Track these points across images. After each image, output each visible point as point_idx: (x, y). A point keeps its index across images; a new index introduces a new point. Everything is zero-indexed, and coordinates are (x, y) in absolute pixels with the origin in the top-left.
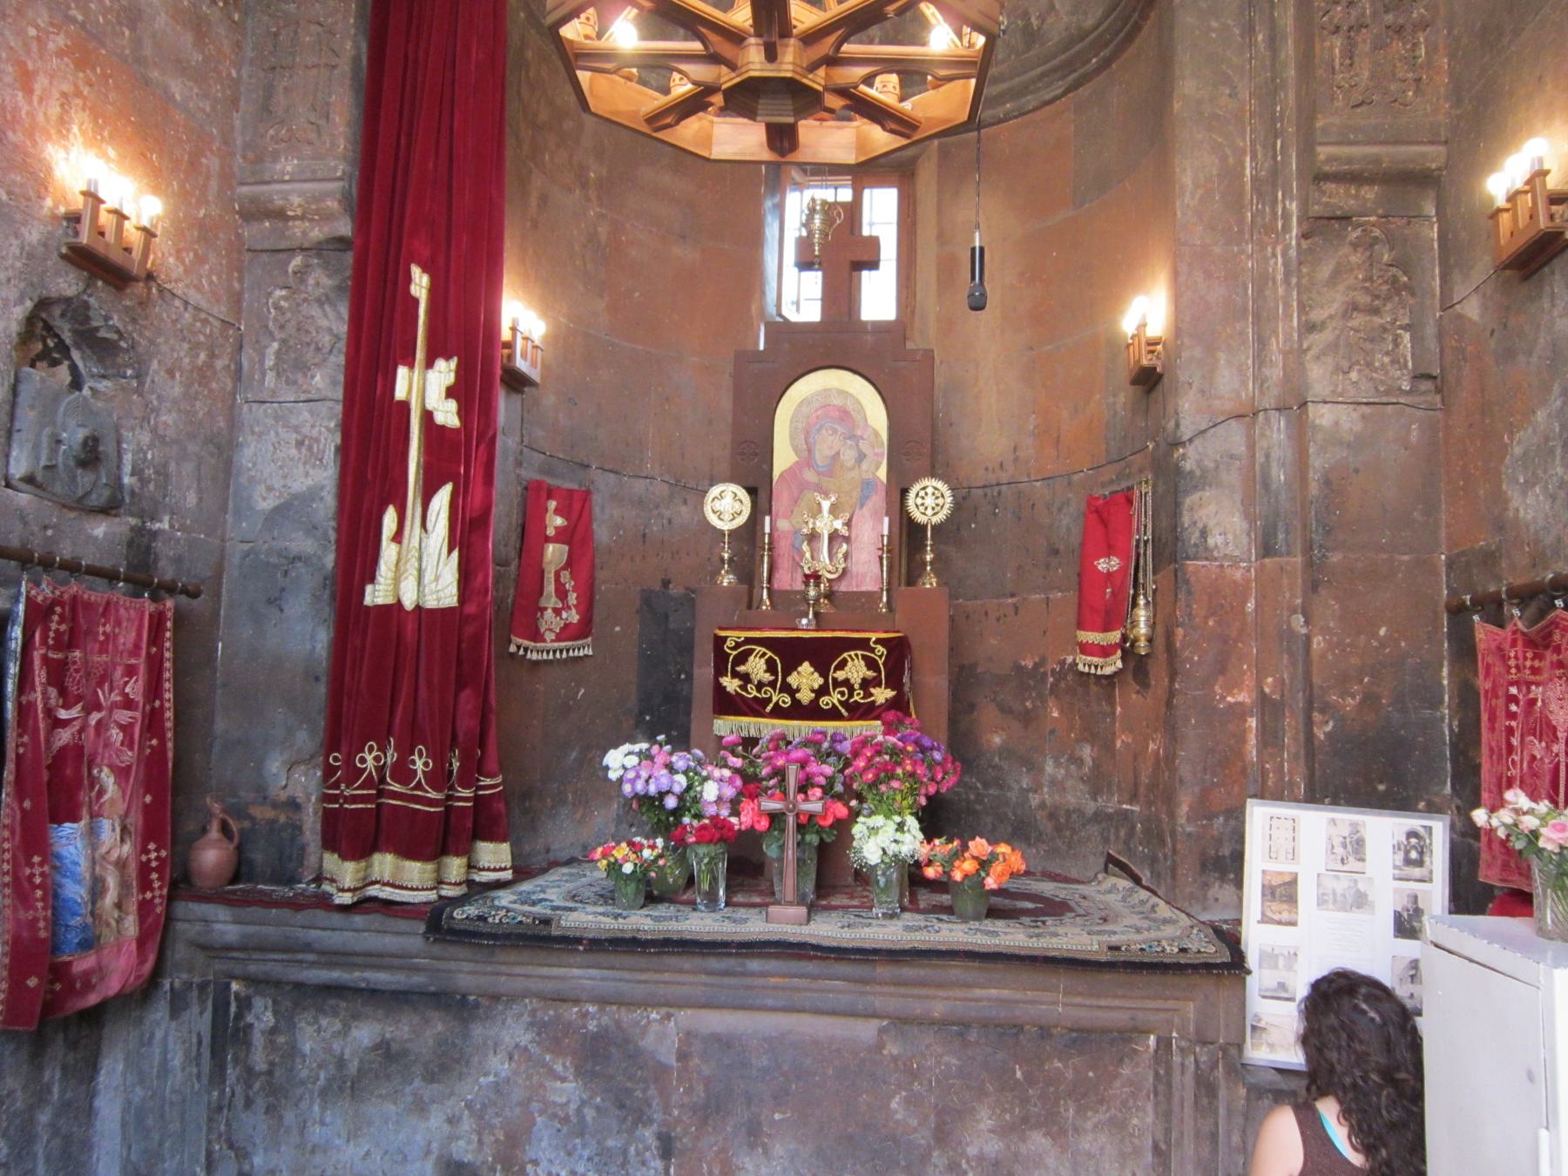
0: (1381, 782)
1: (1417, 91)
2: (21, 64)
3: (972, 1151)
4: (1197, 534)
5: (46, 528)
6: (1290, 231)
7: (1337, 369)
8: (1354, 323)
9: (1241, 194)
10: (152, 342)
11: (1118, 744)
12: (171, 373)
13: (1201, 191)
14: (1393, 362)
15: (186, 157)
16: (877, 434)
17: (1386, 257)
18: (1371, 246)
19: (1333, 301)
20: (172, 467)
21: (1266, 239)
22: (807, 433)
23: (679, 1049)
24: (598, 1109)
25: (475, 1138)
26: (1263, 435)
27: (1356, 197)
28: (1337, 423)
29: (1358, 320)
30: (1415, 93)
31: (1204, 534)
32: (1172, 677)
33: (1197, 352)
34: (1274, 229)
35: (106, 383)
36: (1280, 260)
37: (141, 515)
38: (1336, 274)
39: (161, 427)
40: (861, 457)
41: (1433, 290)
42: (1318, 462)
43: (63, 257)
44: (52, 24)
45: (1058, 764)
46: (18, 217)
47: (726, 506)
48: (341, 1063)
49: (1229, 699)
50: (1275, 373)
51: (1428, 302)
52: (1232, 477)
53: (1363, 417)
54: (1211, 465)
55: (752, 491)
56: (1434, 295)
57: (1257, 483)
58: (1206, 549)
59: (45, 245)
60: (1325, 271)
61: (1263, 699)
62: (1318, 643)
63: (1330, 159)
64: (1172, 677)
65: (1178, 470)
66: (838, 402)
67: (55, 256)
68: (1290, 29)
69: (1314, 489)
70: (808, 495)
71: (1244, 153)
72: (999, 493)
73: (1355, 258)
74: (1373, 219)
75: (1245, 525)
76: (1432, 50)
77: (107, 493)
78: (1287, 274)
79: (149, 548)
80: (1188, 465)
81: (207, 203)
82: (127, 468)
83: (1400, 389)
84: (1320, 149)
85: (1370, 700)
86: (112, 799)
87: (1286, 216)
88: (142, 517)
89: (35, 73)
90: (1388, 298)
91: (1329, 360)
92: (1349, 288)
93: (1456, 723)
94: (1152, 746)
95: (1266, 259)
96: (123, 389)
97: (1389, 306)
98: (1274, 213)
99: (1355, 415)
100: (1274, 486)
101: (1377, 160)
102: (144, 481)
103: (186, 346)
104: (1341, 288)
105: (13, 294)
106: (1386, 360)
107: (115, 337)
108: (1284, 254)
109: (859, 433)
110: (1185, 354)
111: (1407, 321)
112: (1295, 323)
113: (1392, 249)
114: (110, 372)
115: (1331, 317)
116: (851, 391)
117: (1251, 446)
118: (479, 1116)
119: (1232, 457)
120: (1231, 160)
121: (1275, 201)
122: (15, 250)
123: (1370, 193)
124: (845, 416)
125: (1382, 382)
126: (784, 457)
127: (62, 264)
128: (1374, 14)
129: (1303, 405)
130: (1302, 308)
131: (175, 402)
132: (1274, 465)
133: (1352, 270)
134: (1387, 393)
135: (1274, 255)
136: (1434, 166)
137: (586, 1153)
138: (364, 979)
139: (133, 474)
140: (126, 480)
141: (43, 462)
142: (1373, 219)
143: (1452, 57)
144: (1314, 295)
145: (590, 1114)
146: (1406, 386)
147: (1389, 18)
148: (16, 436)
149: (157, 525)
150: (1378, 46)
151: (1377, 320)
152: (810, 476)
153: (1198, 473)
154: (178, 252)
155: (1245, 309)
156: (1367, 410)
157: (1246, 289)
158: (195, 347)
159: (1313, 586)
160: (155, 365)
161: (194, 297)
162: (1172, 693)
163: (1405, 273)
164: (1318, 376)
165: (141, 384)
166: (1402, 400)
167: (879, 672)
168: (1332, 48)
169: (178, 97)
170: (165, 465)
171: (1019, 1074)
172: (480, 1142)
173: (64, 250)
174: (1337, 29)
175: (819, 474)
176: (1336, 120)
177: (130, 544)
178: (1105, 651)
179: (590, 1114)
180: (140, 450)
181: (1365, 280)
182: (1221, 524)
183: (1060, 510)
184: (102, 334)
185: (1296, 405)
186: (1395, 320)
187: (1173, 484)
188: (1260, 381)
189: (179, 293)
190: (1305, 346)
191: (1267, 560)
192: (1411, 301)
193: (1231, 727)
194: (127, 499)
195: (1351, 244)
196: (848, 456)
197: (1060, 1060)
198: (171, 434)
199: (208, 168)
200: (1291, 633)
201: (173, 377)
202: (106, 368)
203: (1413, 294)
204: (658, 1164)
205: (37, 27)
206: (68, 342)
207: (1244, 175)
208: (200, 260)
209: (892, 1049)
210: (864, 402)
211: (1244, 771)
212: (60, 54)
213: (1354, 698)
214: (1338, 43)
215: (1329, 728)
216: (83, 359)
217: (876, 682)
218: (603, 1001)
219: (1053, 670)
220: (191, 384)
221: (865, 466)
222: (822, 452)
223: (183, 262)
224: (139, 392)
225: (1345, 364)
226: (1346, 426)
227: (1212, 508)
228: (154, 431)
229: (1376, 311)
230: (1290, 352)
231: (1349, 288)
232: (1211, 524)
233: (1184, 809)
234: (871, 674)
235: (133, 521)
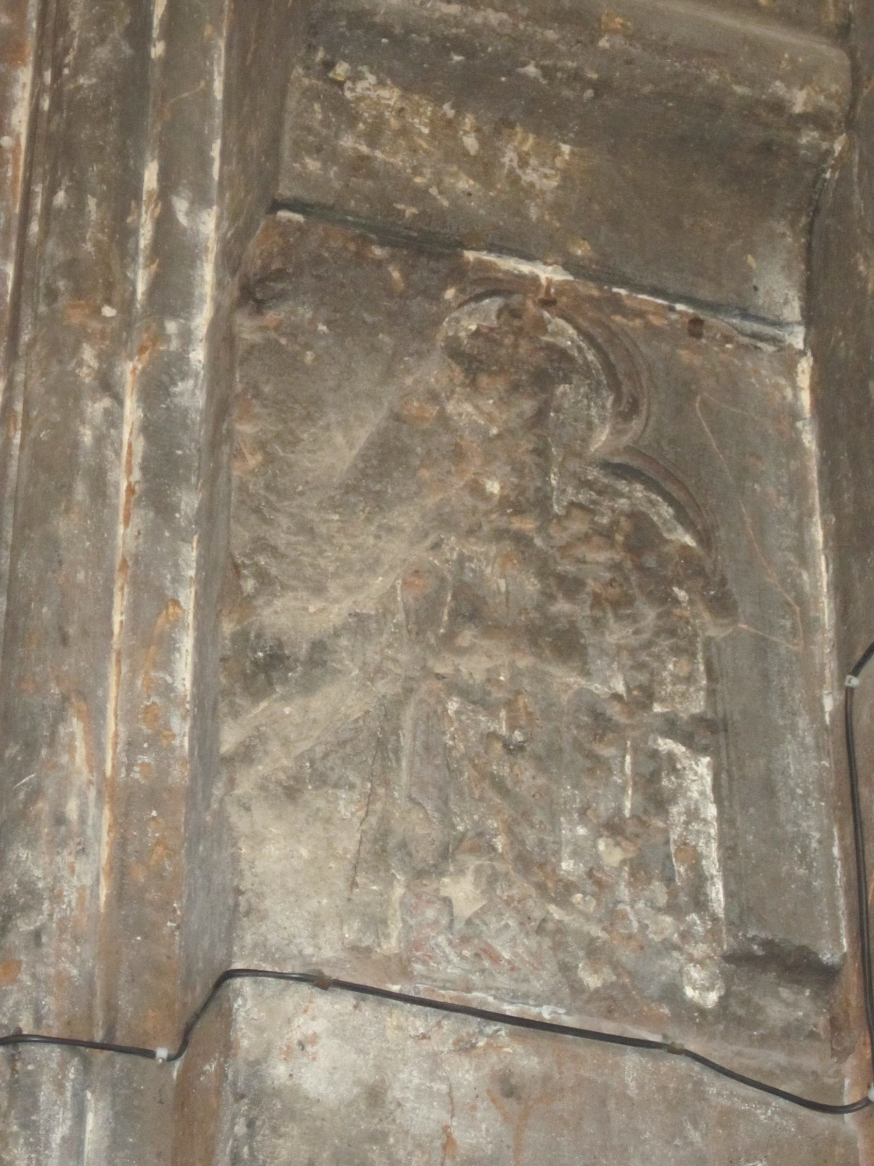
7: (381, 850)
8: (474, 667)
14: (638, 870)
17: (601, 438)
19: (373, 566)
21: (76, 318)
27: (484, 167)
28: (375, 1095)
29: (480, 660)
34: (113, 288)
36: (132, 411)
38: (387, 460)
51: (785, 646)
53: (507, 1087)
56: (808, 626)
60: (337, 448)
74: (548, 273)
78: (161, 472)
83: (672, 993)
91: (346, 806)
92: (443, 520)
95: (70, 395)
97: (616, 634)
98: (122, 233)
104: (407, 518)
106: (611, 854)
108: (156, 389)
111: (697, 705)
112: (183, 675)
113: (628, 409)
115: (359, 625)
121: (126, 192)
123: (541, 166)
129: (204, 1008)
130: (226, 585)
134: (609, 1001)
135: (107, 385)
142: (548, 273)
144: (281, 539)
146: (702, 990)
151: (565, 680)
156: (526, 1059)
163: (683, 517)
164: (293, 876)
181: (513, 505)
186: (644, 696)
190: (230, 738)
192: (713, 629)
195: (454, 351)
203: (722, 605)
226: (420, 1114)
230: (153, 796)
231: (443, 520)
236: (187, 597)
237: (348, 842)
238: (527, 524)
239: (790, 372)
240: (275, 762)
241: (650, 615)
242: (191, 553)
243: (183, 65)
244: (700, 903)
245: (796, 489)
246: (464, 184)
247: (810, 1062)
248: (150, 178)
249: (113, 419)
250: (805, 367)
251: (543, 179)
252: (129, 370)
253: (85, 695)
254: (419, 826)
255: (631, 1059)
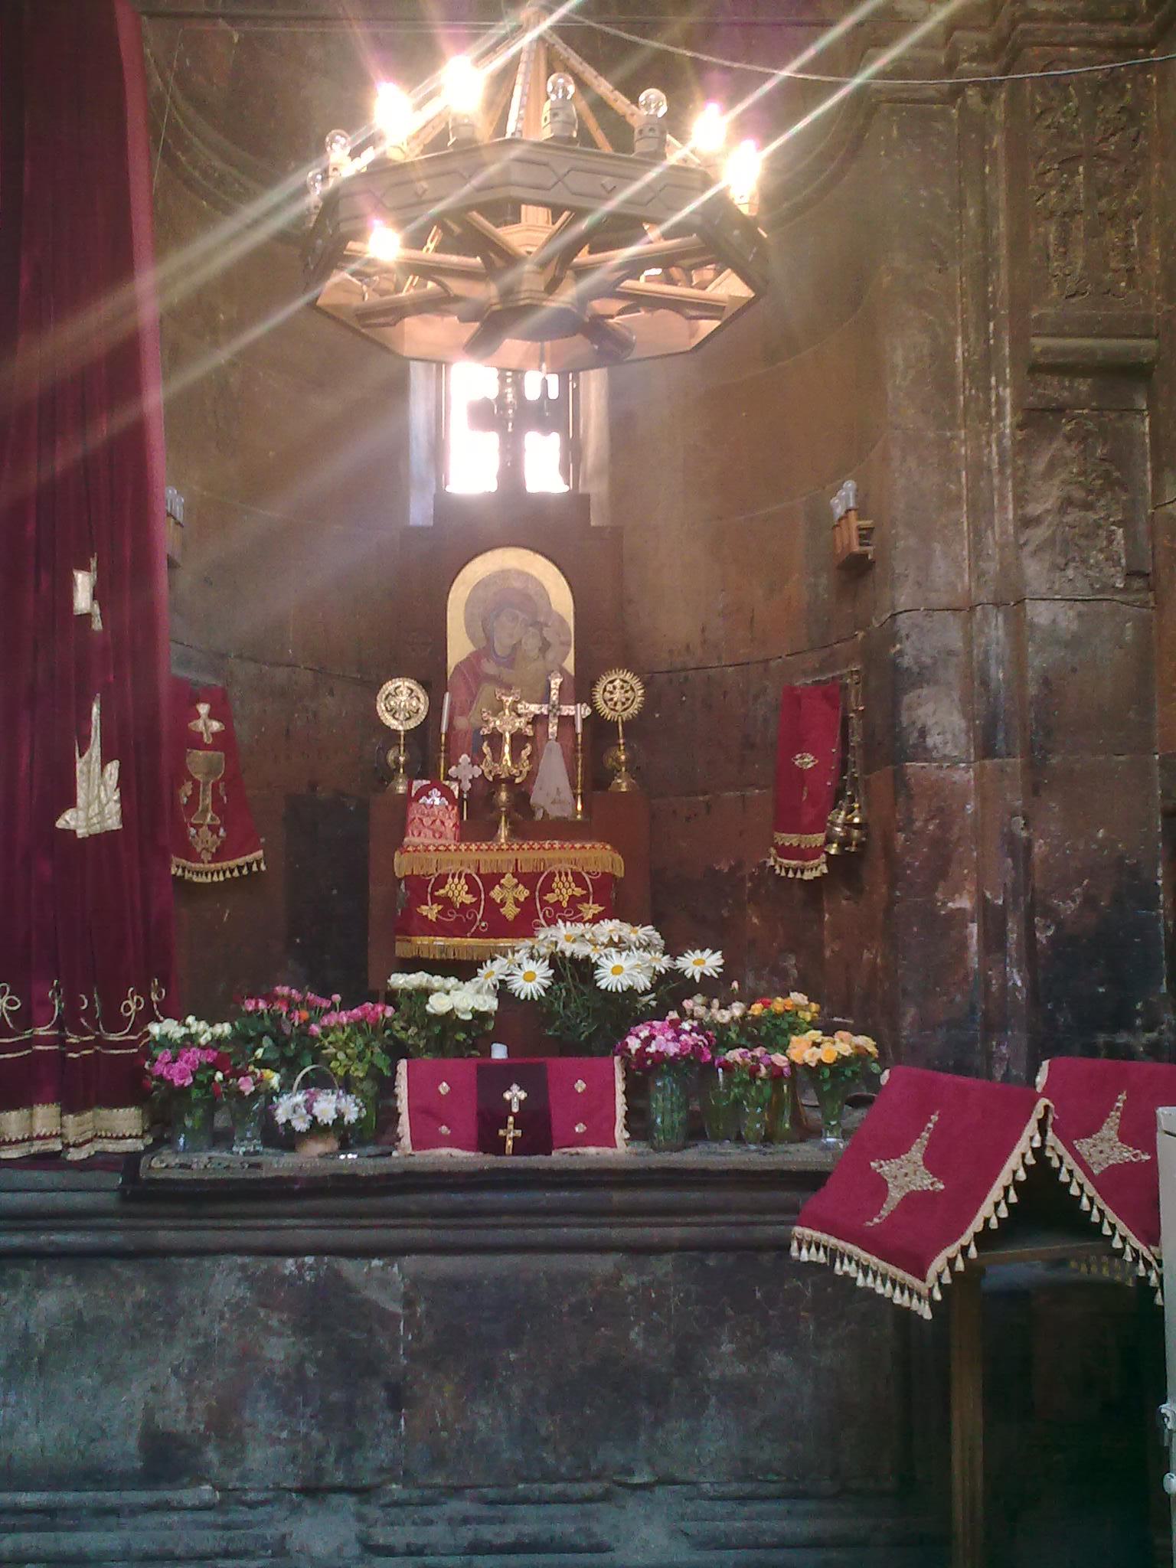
0: (1101, 985)
1: (1131, 284)
3: (714, 1375)
4: (916, 734)
6: (1003, 419)
7: (1056, 568)
9: (953, 375)
11: (828, 953)
13: (912, 373)
16: (562, 621)
18: (1085, 439)
22: (485, 622)
23: (405, 1293)
24: (319, 1363)
25: (183, 1406)
26: (981, 632)
27: (1070, 388)
28: (1054, 621)
29: (1074, 515)
30: (1128, 285)
31: (923, 733)
32: (892, 887)
33: (912, 542)
38: (1051, 467)
40: (545, 646)
41: (1144, 484)
42: (1037, 661)
45: (759, 978)
47: (401, 702)
48: (26, 1338)
49: (950, 904)
50: (992, 567)
52: (951, 674)
53: (1080, 615)
54: (928, 661)
55: (425, 685)
57: (977, 680)
58: (926, 749)
60: (1040, 465)
61: (983, 904)
62: (1039, 847)
63: (1045, 352)
64: (893, 882)
65: (896, 668)
66: (517, 584)
68: (1002, 204)
69: (1032, 690)
70: (487, 690)
71: (956, 335)
72: (686, 678)
73: (1070, 452)
75: (963, 724)
76: (1145, 239)
78: (1002, 464)
80: (906, 661)
84: (1034, 340)
85: (1089, 901)
87: (1000, 402)
90: (1101, 493)
93: (1170, 923)
94: (866, 955)
97: (1102, 502)
99: (1071, 613)
100: (993, 685)
101: (1091, 352)
104: (1057, 482)
106: (1101, 557)
109: (542, 619)
110: (901, 544)
112: (1011, 516)
115: (1048, 511)
116: (535, 573)
117: (969, 640)
118: (187, 1381)
119: (951, 653)
120: (943, 341)
123: (1083, 386)
124: (525, 600)
125: (1098, 580)
126: (459, 647)
128: (1088, 200)
129: (1020, 602)
130: (1020, 500)
132: (992, 662)
133: (1066, 464)
134: (1100, 591)
135: (989, 444)
136: (1145, 360)
137: (309, 1411)
138: (52, 1243)
143: (1164, 247)
145: (311, 1370)
147: (1103, 204)
150: (1093, 232)
151: (1092, 516)
152: (489, 668)
153: (916, 669)
155: (959, 497)
157: (960, 477)
159: (1035, 789)
162: (892, 901)
164: (1034, 570)
166: (1117, 598)
167: (586, 888)
168: (1046, 235)
171: (758, 1295)
172: (190, 1409)
174: (1052, 213)
175: (498, 664)
176: (1050, 310)
178: (815, 852)
179: (311, 1370)
181: (1079, 474)
182: (940, 720)
183: (756, 697)
185: (1012, 601)
187: (891, 681)
188: (979, 575)
191: (987, 762)
193: (953, 933)
196: (531, 645)
197: (798, 1279)
200: (1010, 839)
204: (389, 1416)
207: (955, 357)
209: (631, 1281)
210: (548, 585)
211: (966, 976)
213: (1074, 901)
214: (1052, 232)
215: (1050, 933)
217: (584, 899)
218: (318, 1251)
219: (752, 876)
221: (550, 655)
222: (503, 643)
225: (1061, 561)
226: (1063, 624)
227: (929, 708)
229: (1088, 506)
232: (930, 722)
233: (909, 1019)
234: (579, 892)
236: (1010, 495)
237: (1047, 565)
238: (1082, 479)
239: (1143, 421)
240: (1030, 548)
241: (1109, 494)
242: (1010, 483)
243: (998, 348)
244: (1120, 564)
245: (1144, 455)
246: (1066, 394)
247: (1141, 596)
248: (993, 380)
249: (990, 452)
250: (1147, 420)
251: (1084, 388)
252: (994, 435)
253: (991, 524)
254: (1061, 561)
255: (1105, 603)
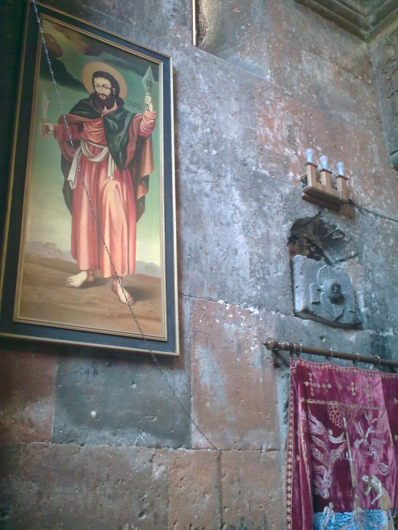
2: (265, 117)
5: (322, 338)
10: (361, 236)
12: (375, 250)
15: (358, 146)
20: (388, 301)
35: (344, 263)
37: (375, 328)
39: (376, 280)
43: (304, 198)
44: (277, 98)
46: (277, 182)
59: (293, 194)
67: (300, 199)
77: (352, 316)
79: (384, 347)
81: (375, 165)
82: (362, 303)
86: (382, 496)
88: (376, 329)
89: (273, 119)
96: (352, 263)
102: (373, 310)
103: (381, 237)
105: (281, 218)
107: (341, 236)
114: (344, 257)
122: (278, 198)
127: (304, 202)
131: (381, 265)
139: (366, 306)
140: (363, 310)
141: (311, 301)
148: (296, 290)
149: (386, 334)
154: (365, 190)
158: (386, 237)
160: (365, 248)
161: (378, 210)
165: (361, 258)
169: (347, 120)
170: (384, 300)
173: (303, 194)
177: (372, 344)
180: (366, 293)
184: (335, 237)
189: (371, 210)
194: (365, 320)
198: (383, 282)
199: (372, 150)
201: (377, 253)
202: (342, 256)
205: (270, 100)
206: (321, 247)
208: (379, 193)
212: (283, 109)
216: (330, 254)
220: (389, 256)
223: (369, 195)
224: (360, 262)
228: (373, 282)
235: (371, 332)
